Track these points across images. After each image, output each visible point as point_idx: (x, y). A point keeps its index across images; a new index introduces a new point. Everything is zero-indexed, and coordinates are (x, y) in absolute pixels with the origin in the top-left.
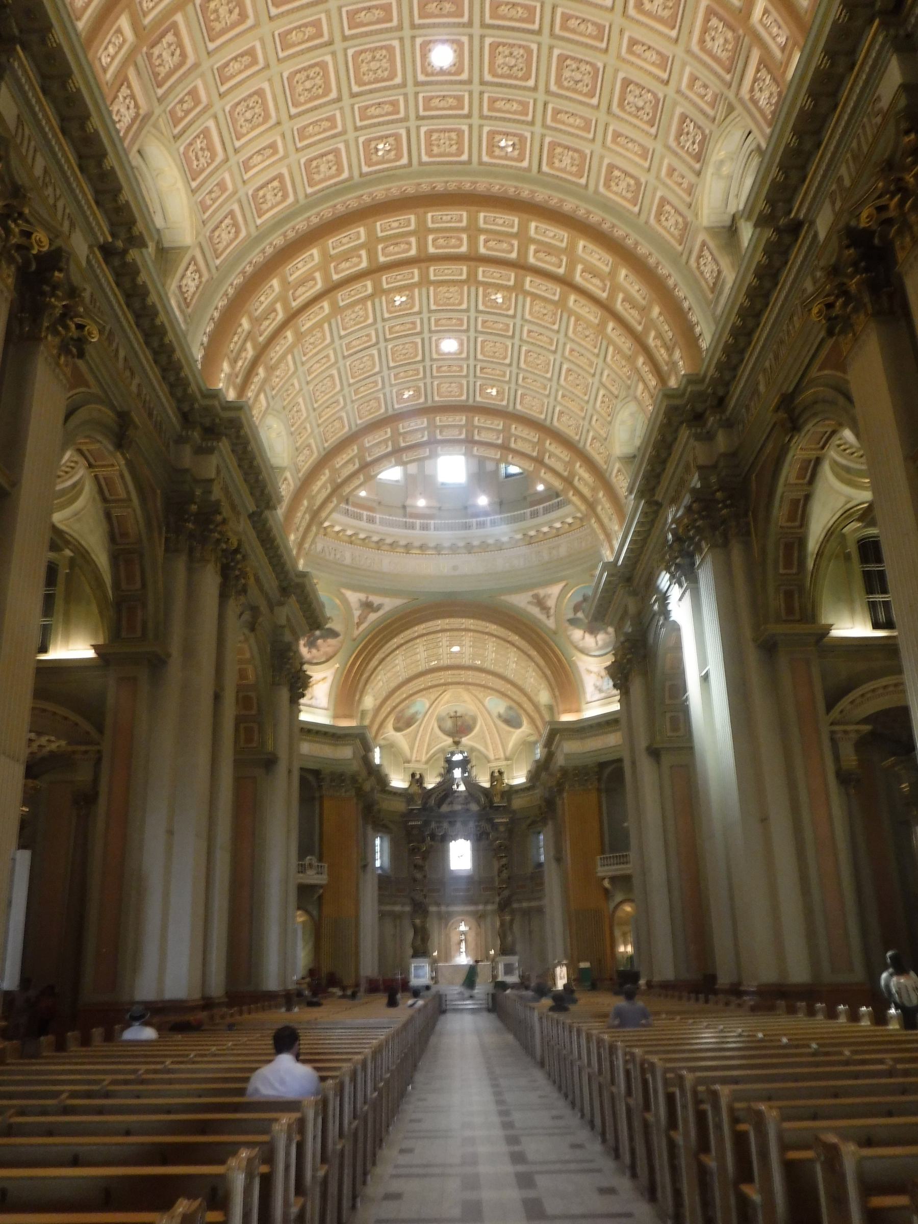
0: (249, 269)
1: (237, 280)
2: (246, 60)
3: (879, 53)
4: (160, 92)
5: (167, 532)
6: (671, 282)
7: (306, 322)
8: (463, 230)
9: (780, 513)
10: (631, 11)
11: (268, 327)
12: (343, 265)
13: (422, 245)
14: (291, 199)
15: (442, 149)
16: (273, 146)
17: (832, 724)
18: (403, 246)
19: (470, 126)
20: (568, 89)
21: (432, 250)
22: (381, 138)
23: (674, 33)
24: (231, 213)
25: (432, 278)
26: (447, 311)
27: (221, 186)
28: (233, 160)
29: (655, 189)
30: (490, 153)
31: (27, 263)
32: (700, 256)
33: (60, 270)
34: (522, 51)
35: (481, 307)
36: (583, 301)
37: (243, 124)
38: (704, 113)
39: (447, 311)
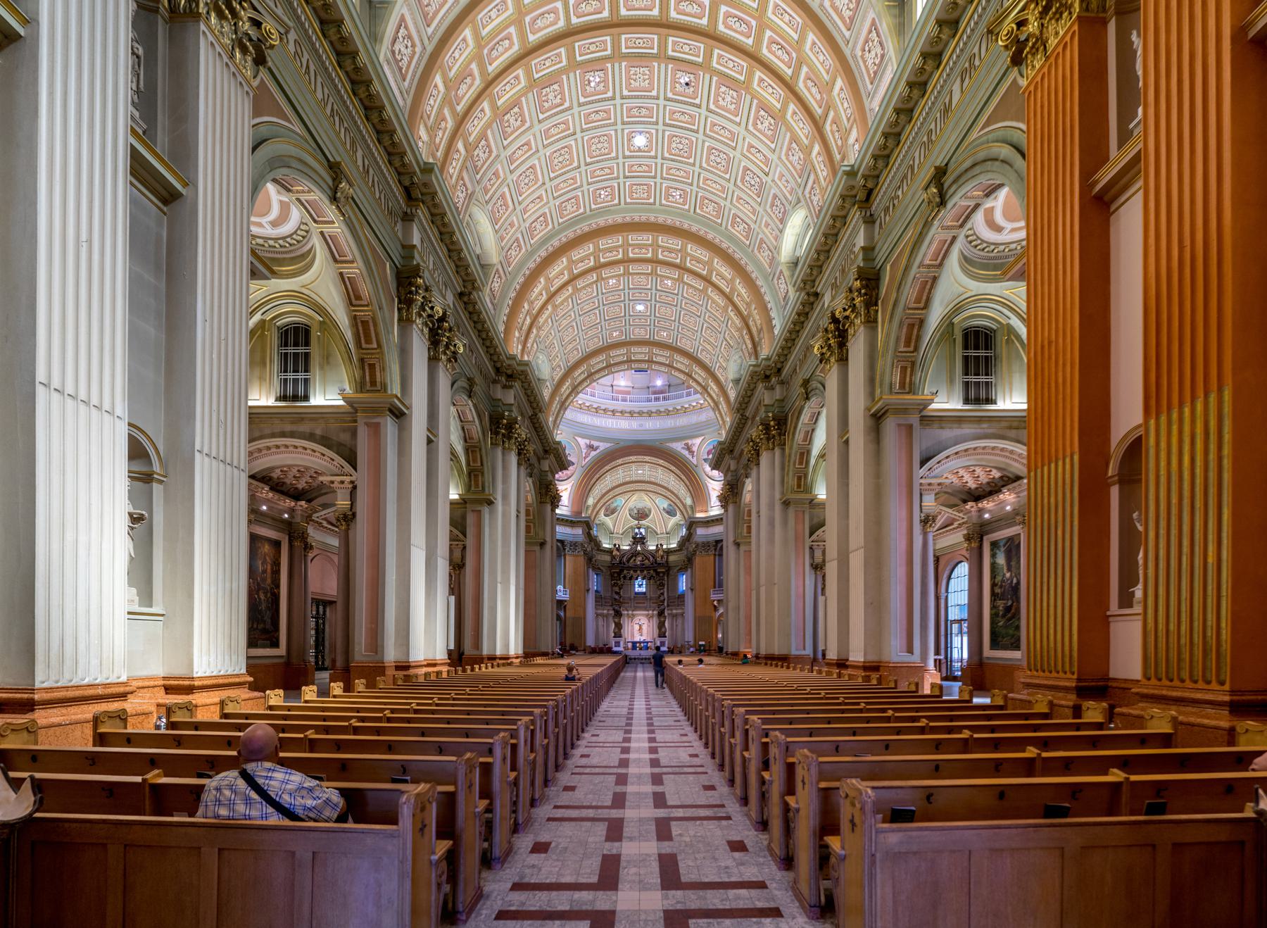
0: (527, 272)
1: (521, 279)
2: (526, 148)
3: (856, 222)
4: (478, 177)
6: (763, 290)
7: (559, 299)
8: (650, 245)
10: (750, 128)
11: (538, 304)
12: (580, 265)
13: (625, 252)
14: (550, 227)
15: (638, 196)
18: (615, 253)
19: (655, 183)
20: (713, 167)
21: (631, 255)
22: (603, 188)
23: (773, 146)
24: (517, 239)
25: (631, 271)
26: (639, 289)
27: (512, 225)
28: (518, 208)
29: (758, 233)
30: (667, 199)
31: (434, 325)
32: (779, 278)
33: (446, 322)
34: (687, 141)
35: (659, 288)
36: (716, 292)
39: (639, 289)
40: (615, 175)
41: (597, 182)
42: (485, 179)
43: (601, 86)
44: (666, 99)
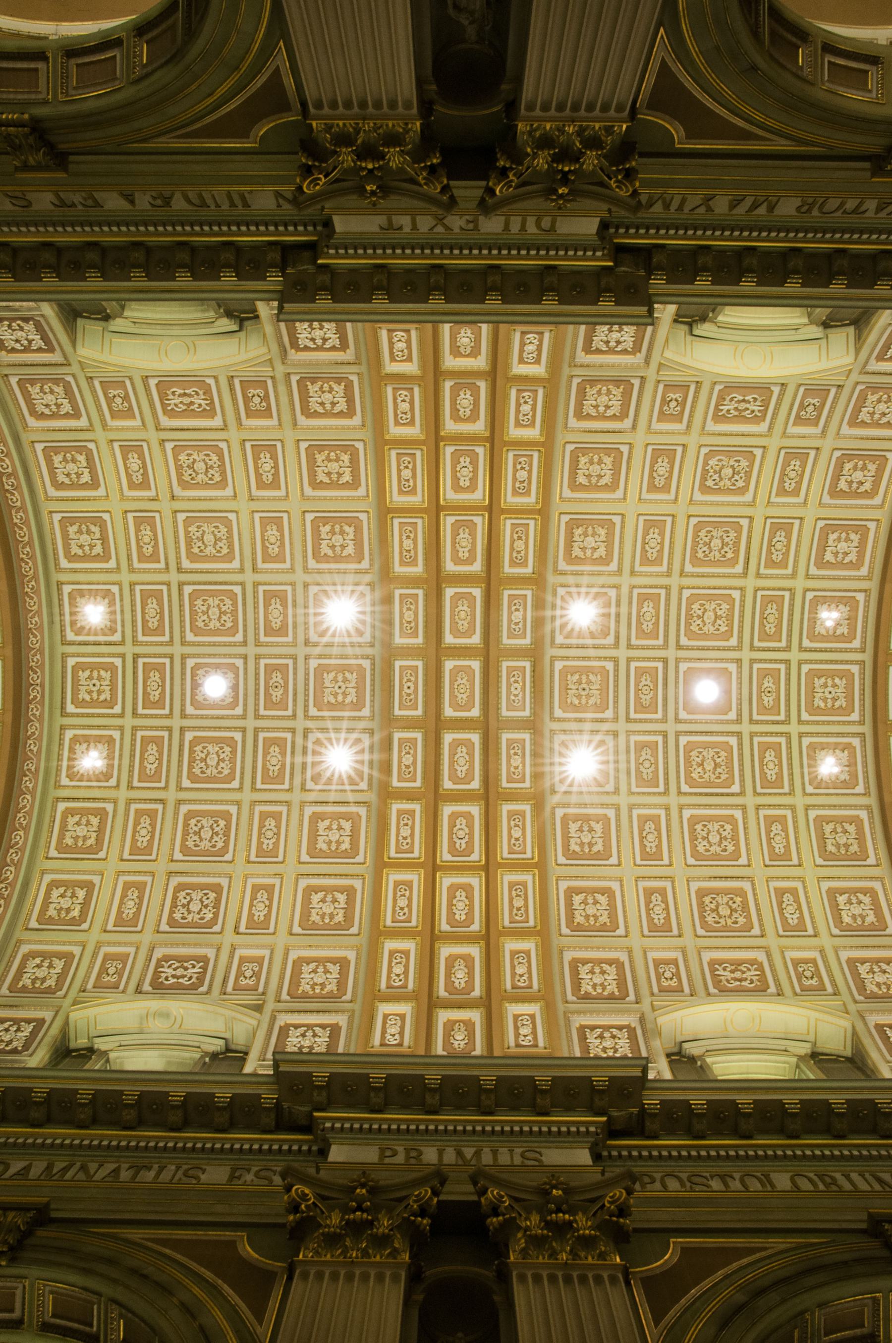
14: (52, 492)
16: (145, 484)
37: (191, 458)
38: (225, 980)
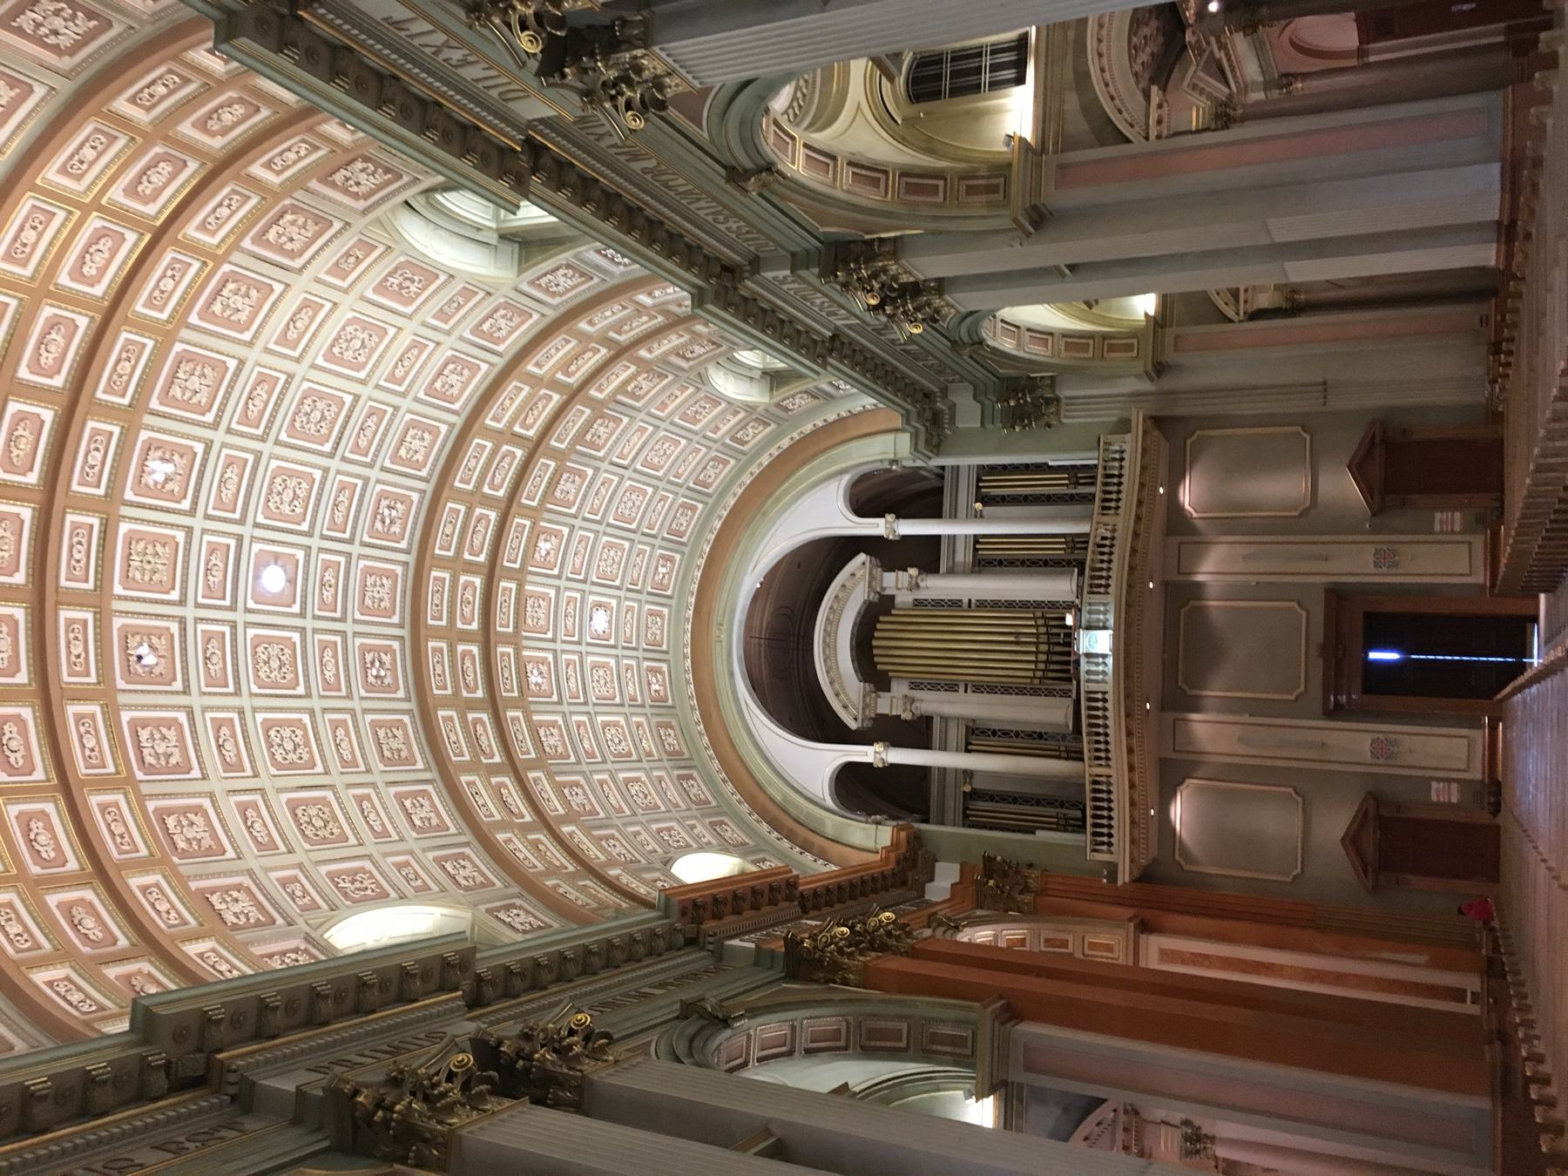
4: (280, 921)
5: (835, 982)
9: (869, 197)
17: (1147, 138)
20: (331, 430)
22: (365, 671)
28: (370, 848)
31: (489, 1080)
40: (338, 639)
41: (348, 682)
42: (293, 910)
43: (160, 643)
44: (192, 512)
